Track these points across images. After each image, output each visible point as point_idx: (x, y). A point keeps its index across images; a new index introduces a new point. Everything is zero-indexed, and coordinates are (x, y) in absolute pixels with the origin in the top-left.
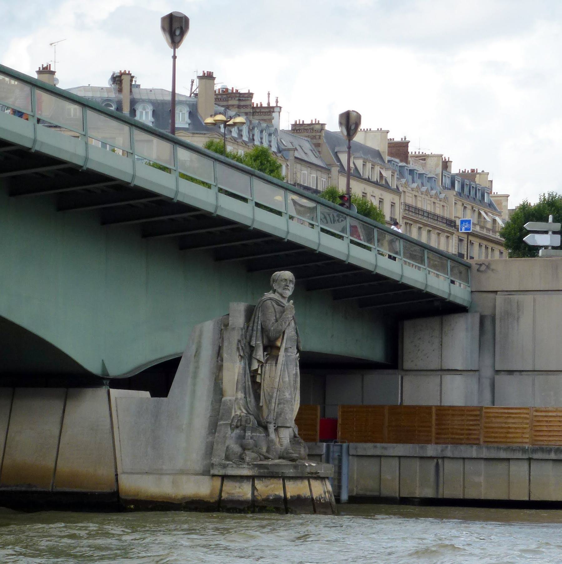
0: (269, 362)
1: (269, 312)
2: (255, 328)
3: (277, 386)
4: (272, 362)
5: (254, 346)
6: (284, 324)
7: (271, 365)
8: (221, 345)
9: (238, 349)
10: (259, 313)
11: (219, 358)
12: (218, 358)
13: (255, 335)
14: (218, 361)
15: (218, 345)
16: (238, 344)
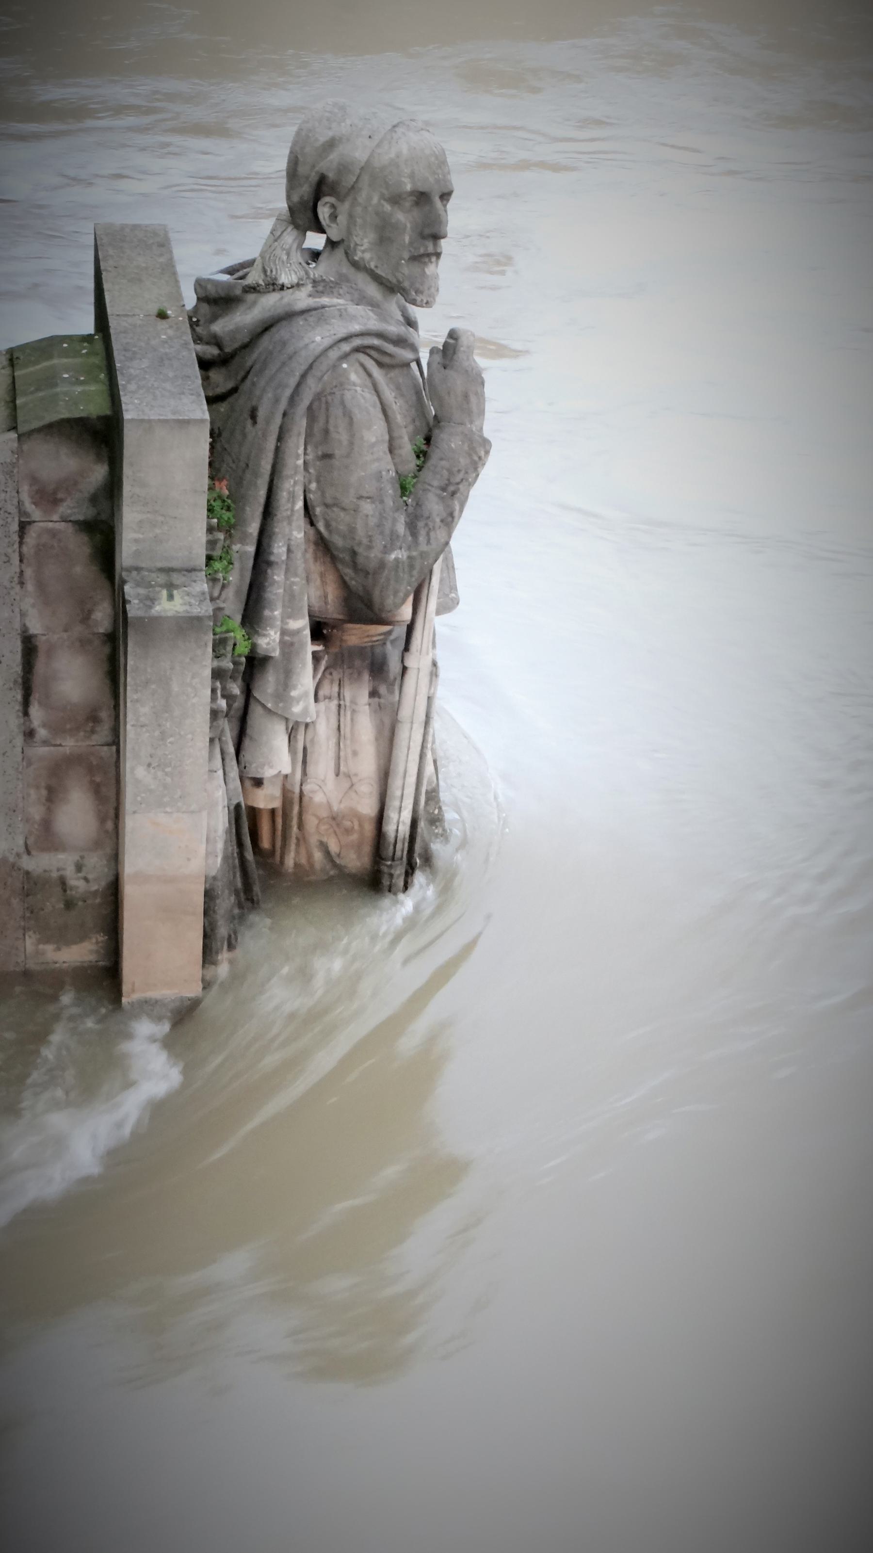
0: (323, 692)
1: (373, 445)
2: (279, 550)
3: (406, 845)
4: (347, 694)
5: (276, 654)
6: (456, 514)
7: (339, 706)
8: (35, 627)
9: (215, 714)
10: (298, 448)
11: (35, 711)
12: (26, 714)
13: (281, 591)
14: (30, 734)
15: (17, 625)
16: (213, 691)
